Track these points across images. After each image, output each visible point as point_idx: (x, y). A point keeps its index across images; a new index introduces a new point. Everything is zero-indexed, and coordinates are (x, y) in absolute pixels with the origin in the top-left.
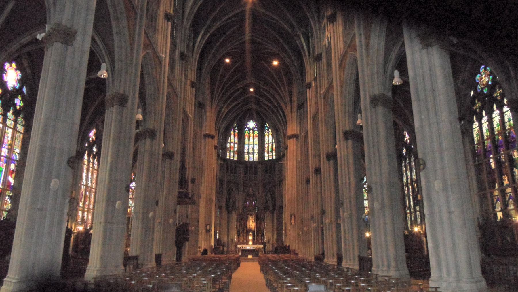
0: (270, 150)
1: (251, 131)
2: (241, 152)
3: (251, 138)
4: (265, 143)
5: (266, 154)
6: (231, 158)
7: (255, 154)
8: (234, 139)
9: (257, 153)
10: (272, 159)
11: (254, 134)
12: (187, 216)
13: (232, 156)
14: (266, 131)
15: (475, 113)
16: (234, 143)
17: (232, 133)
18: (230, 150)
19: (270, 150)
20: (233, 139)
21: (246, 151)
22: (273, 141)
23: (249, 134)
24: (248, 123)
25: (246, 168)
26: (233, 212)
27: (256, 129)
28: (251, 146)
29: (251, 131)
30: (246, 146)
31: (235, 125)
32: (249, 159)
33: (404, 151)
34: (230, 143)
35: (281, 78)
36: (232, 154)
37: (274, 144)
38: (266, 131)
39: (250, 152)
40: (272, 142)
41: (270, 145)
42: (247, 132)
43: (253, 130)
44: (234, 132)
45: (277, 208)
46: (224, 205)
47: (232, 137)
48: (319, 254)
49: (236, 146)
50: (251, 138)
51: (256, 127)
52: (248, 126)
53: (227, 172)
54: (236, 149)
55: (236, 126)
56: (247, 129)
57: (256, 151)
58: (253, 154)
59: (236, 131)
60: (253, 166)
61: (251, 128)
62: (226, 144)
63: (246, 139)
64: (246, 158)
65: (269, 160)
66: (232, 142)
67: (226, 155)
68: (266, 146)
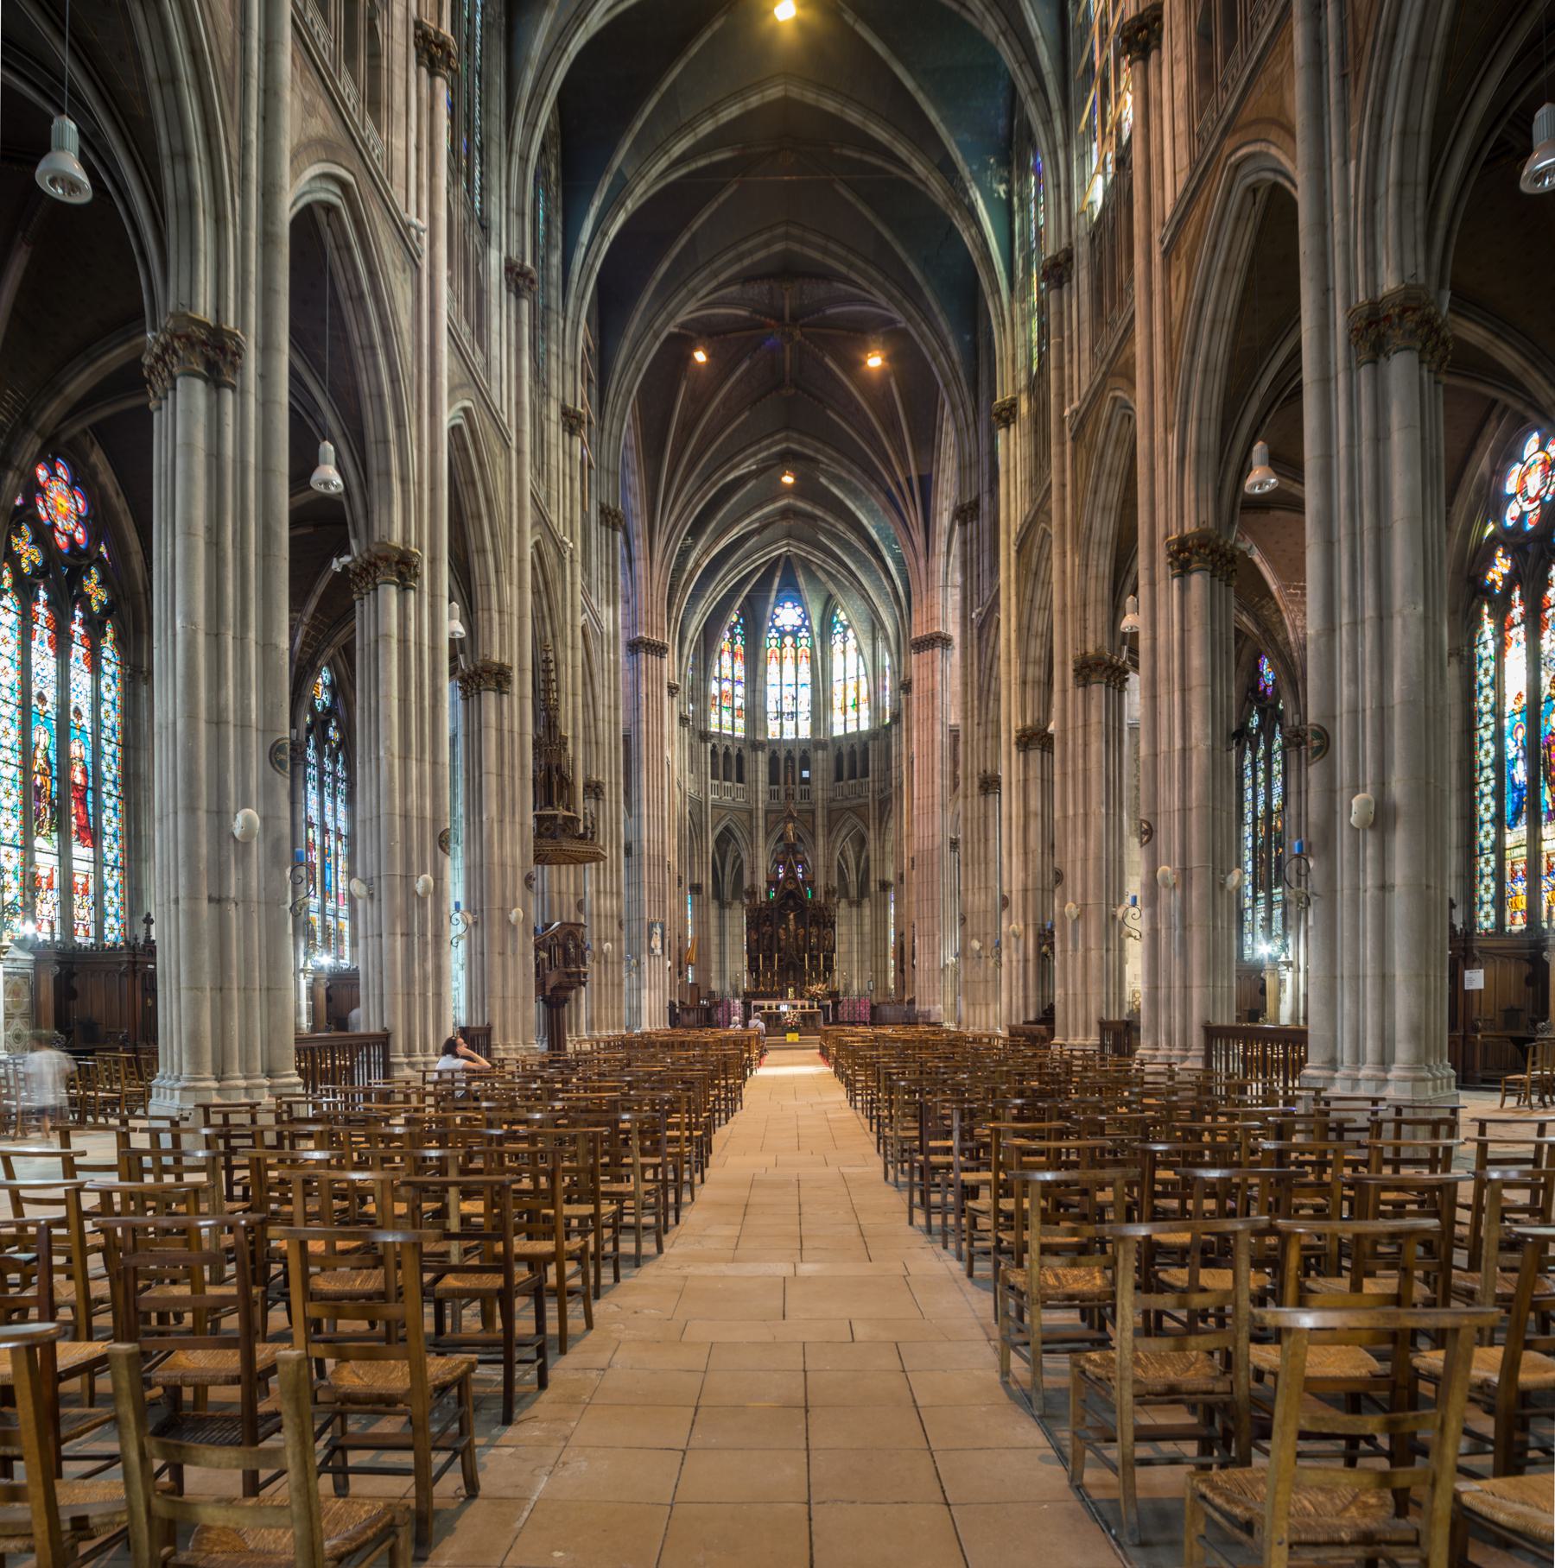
0: (850, 702)
1: (789, 640)
2: (754, 713)
3: (789, 665)
4: (835, 678)
5: (837, 717)
7: (801, 717)
10: (859, 734)
11: (796, 649)
12: (580, 906)
13: (726, 722)
14: (838, 637)
15: (1485, 592)
17: (725, 645)
19: (850, 702)
20: (728, 665)
21: (771, 707)
22: (862, 671)
23: (781, 649)
24: (778, 611)
25: (773, 761)
27: (804, 633)
28: (789, 691)
29: (789, 640)
30: (772, 693)
31: (734, 618)
32: (781, 733)
33: (1255, 721)
34: (720, 680)
35: (892, 426)
36: (726, 716)
37: (863, 680)
38: (838, 637)
39: (786, 709)
41: (851, 684)
43: (794, 634)
44: (733, 644)
45: (873, 886)
47: (726, 658)
48: (1026, 1023)
49: (740, 690)
50: (789, 665)
51: (803, 626)
52: (778, 623)
54: (739, 702)
55: (737, 623)
56: (774, 633)
57: (805, 707)
58: (794, 715)
59: (739, 639)
60: (797, 755)
61: (788, 628)
62: (706, 680)
63: (773, 667)
64: (773, 730)
65: (847, 736)
67: (706, 720)
68: (838, 688)
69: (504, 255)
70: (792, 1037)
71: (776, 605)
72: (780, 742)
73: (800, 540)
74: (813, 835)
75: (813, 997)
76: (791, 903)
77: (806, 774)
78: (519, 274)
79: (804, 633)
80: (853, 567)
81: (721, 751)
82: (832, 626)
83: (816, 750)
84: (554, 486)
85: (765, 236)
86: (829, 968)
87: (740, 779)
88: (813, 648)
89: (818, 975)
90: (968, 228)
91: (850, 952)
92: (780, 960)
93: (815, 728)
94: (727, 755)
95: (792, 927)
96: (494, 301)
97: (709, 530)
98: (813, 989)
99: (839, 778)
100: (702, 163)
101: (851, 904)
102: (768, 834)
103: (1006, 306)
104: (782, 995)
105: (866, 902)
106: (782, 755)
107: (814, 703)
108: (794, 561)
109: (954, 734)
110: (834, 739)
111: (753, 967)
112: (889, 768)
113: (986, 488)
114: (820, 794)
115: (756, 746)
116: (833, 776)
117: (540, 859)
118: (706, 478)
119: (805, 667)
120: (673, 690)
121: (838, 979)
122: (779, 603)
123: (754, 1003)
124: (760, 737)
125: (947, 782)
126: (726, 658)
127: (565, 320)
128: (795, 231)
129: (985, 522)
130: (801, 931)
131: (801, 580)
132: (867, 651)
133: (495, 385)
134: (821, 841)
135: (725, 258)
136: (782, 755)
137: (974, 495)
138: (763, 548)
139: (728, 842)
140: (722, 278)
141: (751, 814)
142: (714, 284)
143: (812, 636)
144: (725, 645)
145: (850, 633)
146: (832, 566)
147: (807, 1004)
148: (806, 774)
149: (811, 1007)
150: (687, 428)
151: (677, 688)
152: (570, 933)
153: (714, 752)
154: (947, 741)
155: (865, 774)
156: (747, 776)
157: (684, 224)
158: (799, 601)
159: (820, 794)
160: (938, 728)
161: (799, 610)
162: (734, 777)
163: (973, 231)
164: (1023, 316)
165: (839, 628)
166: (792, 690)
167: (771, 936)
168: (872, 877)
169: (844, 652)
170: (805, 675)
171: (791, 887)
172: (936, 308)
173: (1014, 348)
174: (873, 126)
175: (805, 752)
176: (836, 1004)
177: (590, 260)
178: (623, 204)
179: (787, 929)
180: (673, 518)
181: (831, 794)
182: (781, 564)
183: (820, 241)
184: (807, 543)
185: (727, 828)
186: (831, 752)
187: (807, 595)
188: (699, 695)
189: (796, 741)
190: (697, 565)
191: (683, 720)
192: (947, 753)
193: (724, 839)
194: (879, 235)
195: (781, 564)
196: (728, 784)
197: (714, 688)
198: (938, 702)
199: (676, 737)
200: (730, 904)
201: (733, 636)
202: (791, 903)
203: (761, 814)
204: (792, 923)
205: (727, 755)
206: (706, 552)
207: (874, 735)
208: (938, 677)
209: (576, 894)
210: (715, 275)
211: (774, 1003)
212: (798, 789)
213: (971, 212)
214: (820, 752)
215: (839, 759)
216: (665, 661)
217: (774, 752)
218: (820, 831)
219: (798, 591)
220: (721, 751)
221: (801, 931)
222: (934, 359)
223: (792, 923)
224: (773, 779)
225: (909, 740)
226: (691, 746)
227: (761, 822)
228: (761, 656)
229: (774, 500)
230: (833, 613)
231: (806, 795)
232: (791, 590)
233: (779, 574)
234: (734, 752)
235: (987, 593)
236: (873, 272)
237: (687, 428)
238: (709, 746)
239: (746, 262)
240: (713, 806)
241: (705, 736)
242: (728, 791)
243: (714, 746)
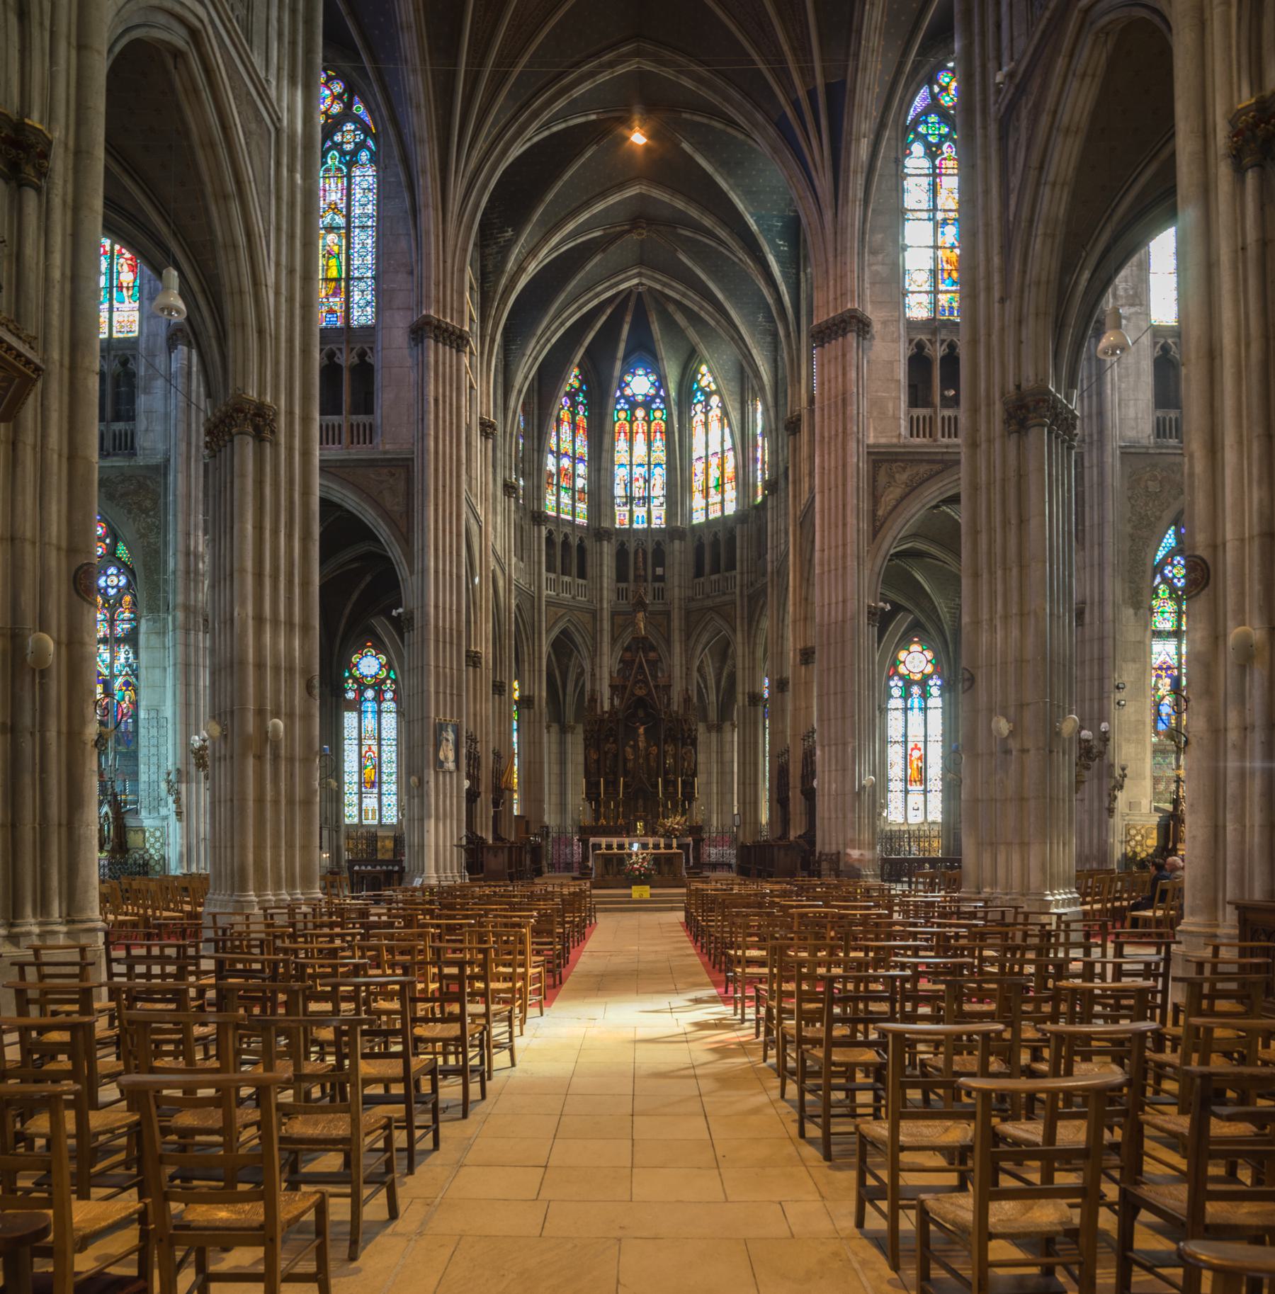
0: (712, 483)
1: (640, 413)
2: (599, 495)
3: (640, 440)
4: (695, 456)
5: (698, 501)
6: (563, 516)
8: (574, 441)
9: (662, 499)
10: (724, 519)
11: (649, 423)
14: (699, 407)
16: (575, 459)
18: (558, 485)
19: (712, 483)
21: (619, 491)
22: (728, 444)
23: (631, 423)
24: (628, 378)
27: (658, 403)
29: (640, 413)
30: (621, 473)
36: (566, 499)
37: (730, 456)
38: (699, 407)
39: (637, 494)
40: (723, 452)
42: (622, 415)
43: (647, 404)
44: (574, 415)
47: (566, 429)
49: (581, 469)
50: (640, 440)
51: (657, 395)
52: (628, 392)
54: (580, 483)
55: (580, 390)
56: (622, 404)
57: (658, 491)
58: (647, 500)
59: (581, 411)
60: (650, 548)
61: (640, 398)
63: (621, 445)
64: (621, 517)
65: (709, 523)
66: (566, 455)
67: (540, 498)
68: (699, 467)
70: (640, 892)
71: (625, 371)
72: (630, 532)
73: (654, 268)
74: (668, 641)
75: (669, 834)
76: (641, 713)
77: (659, 571)
79: (658, 403)
80: (720, 296)
81: (559, 539)
82: (692, 394)
83: (672, 541)
86: (689, 796)
87: (582, 574)
88: (668, 422)
89: (675, 805)
91: (709, 783)
92: (626, 785)
93: (670, 514)
94: (566, 544)
95: (641, 745)
97: (535, 218)
98: (669, 822)
99: (699, 572)
104: (629, 831)
106: (632, 547)
107: (670, 485)
108: (648, 300)
110: (693, 528)
111: (592, 794)
114: (676, 593)
119: (659, 444)
121: (698, 811)
122: (629, 369)
123: (592, 840)
126: (566, 429)
130: (654, 750)
131: (656, 328)
132: (735, 416)
134: (677, 648)
138: (608, 278)
141: (595, 615)
143: (668, 407)
144: (565, 415)
145: (715, 400)
146: (693, 302)
147: (662, 842)
148: (659, 571)
149: (669, 846)
153: (550, 541)
155: (731, 566)
156: (590, 571)
158: (654, 366)
159: (676, 593)
161: (652, 378)
162: (574, 570)
165: (700, 396)
166: (643, 470)
167: (616, 756)
168: (739, 689)
169: (706, 424)
170: (660, 454)
171: (640, 692)
175: (658, 544)
176: (698, 842)
179: (635, 747)
182: (631, 305)
185: (564, 632)
187: (662, 349)
188: (530, 463)
189: (648, 531)
193: (563, 647)
195: (631, 305)
196: (566, 579)
197: (551, 463)
201: (574, 405)
202: (641, 713)
203: (606, 615)
204: (642, 738)
205: (566, 544)
211: (615, 841)
214: (677, 542)
215: (699, 550)
217: (622, 544)
218: (676, 636)
220: (559, 539)
221: (654, 750)
223: (642, 738)
224: (621, 576)
227: (606, 625)
228: (608, 427)
229: (621, 186)
230: (694, 379)
232: (644, 353)
233: (628, 319)
234: (574, 541)
238: (544, 532)
240: (549, 604)
241: (538, 518)
242: (567, 587)
243: (550, 532)
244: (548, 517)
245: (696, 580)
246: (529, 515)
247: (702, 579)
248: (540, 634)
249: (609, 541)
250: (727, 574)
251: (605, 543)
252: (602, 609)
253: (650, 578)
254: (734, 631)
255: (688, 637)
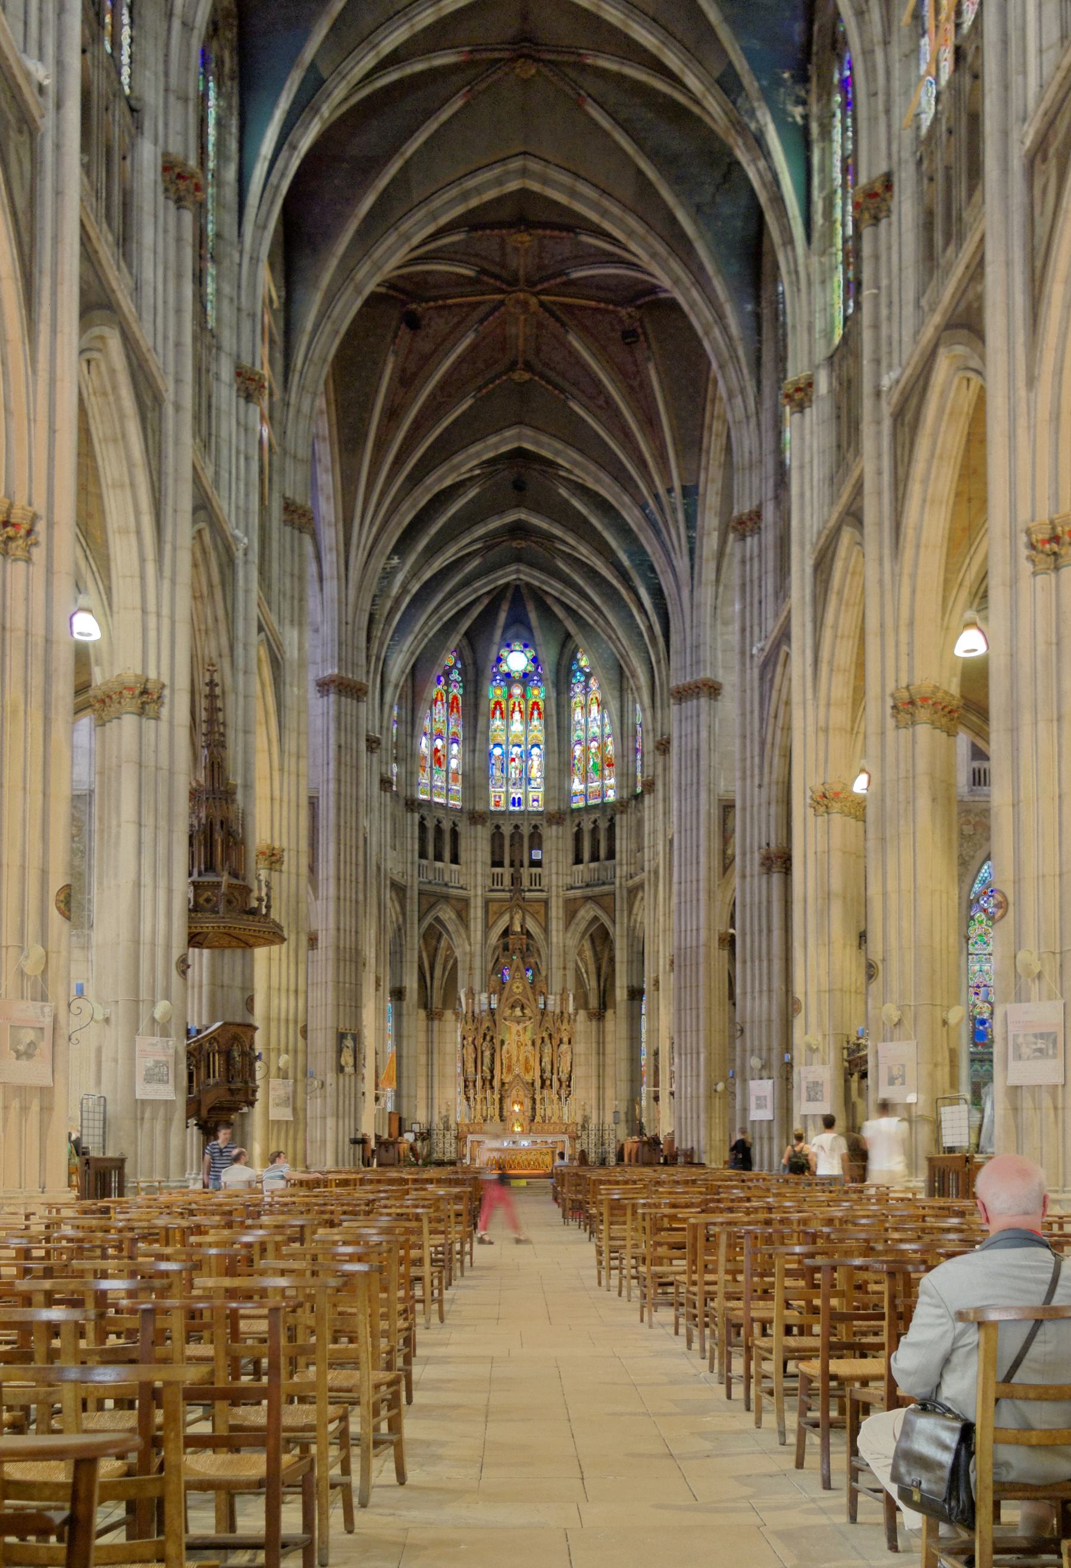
10: (604, 806)
25: (497, 837)
26: (449, 1014)
31: (450, 660)
46: (411, 983)
53: (423, 855)
60: (526, 831)
69: (159, 151)
74: (546, 930)
78: (180, 176)
81: (430, 824)
84: (224, 464)
85: (497, 171)
90: (754, 161)
96: (147, 207)
100: (419, 67)
101: (590, 1016)
102: (487, 927)
103: (801, 260)
105: (609, 1013)
106: (507, 830)
109: (727, 808)
112: (640, 849)
113: (770, 494)
115: (476, 818)
116: (571, 858)
117: (195, 940)
118: (415, 479)
120: (373, 744)
124: (480, 807)
125: (716, 862)
127: (241, 252)
128: (535, 166)
129: (769, 537)
133: (147, 316)
135: (446, 197)
136: (507, 830)
137: (755, 503)
139: (440, 937)
140: (443, 220)
142: (431, 229)
148: (537, 855)
150: (392, 414)
151: (378, 742)
152: (236, 1038)
153: (422, 827)
154: (715, 812)
155: (611, 855)
156: (463, 856)
157: (395, 150)
160: (704, 796)
162: (447, 855)
163: (762, 164)
164: (823, 272)
172: (710, 268)
173: (811, 313)
174: (636, 26)
177: (274, 179)
178: (316, 111)
180: (374, 530)
181: (569, 880)
183: (565, 179)
184: (541, 569)
186: (570, 830)
190: (404, 589)
191: (385, 783)
192: (716, 827)
194: (640, 173)
196: (439, 864)
197: (424, 745)
198: (703, 763)
199: (376, 804)
200: (440, 1016)
203: (479, 902)
206: (414, 574)
207: (621, 806)
208: (704, 734)
209: (243, 989)
210: (434, 216)
212: (526, 872)
213: (759, 141)
214: (554, 827)
216: (363, 707)
219: (530, 629)
222: (707, 333)
225: (666, 813)
226: (393, 815)
231: (536, 880)
234: (446, 826)
235: (770, 623)
236: (632, 222)
237: (392, 414)
238: (417, 816)
239: (474, 203)
241: (412, 804)
243: (423, 818)
244: (421, 804)
245: (575, 867)
246: (402, 802)
247: (581, 867)
248: (412, 924)
249: (483, 824)
250: (607, 863)
251: (479, 827)
252: (476, 896)
253: (526, 862)
254: (614, 922)
255: (567, 927)
